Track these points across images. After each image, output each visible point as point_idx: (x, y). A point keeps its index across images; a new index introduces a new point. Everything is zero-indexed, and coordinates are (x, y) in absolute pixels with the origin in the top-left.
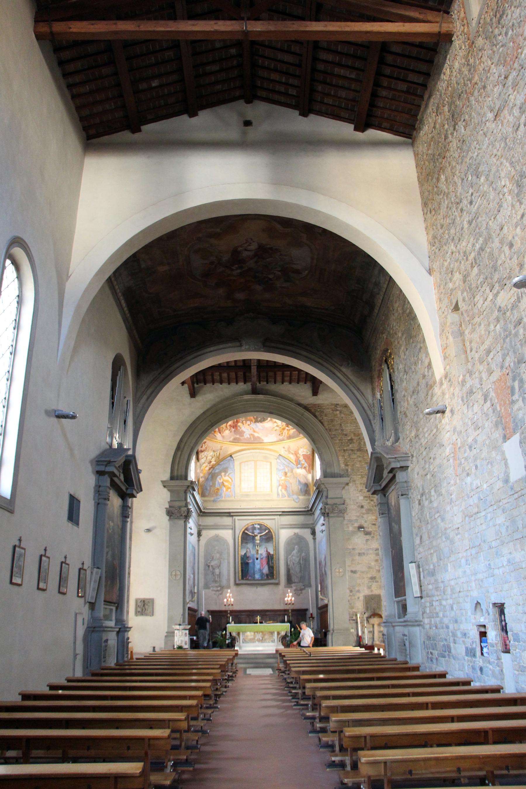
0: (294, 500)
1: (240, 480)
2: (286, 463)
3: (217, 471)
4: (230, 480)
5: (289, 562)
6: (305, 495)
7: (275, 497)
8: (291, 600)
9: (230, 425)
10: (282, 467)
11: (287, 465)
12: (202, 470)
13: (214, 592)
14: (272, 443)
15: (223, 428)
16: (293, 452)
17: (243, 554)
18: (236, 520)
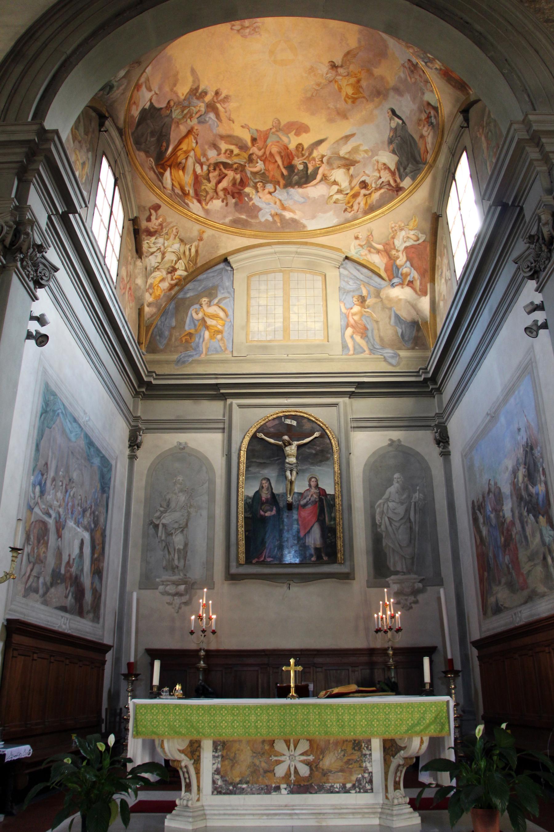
0: (385, 360)
1: (248, 312)
2: (361, 277)
3: (190, 294)
4: (222, 314)
5: (378, 518)
6: (413, 349)
7: (337, 350)
8: (393, 617)
9: (225, 190)
10: (352, 285)
11: (366, 280)
12: (151, 286)
13: (168, 599)
14: (328, 231)
15: (207, 193)
16: (380, 247)
17: (251, 494)
18: (235, 408)
